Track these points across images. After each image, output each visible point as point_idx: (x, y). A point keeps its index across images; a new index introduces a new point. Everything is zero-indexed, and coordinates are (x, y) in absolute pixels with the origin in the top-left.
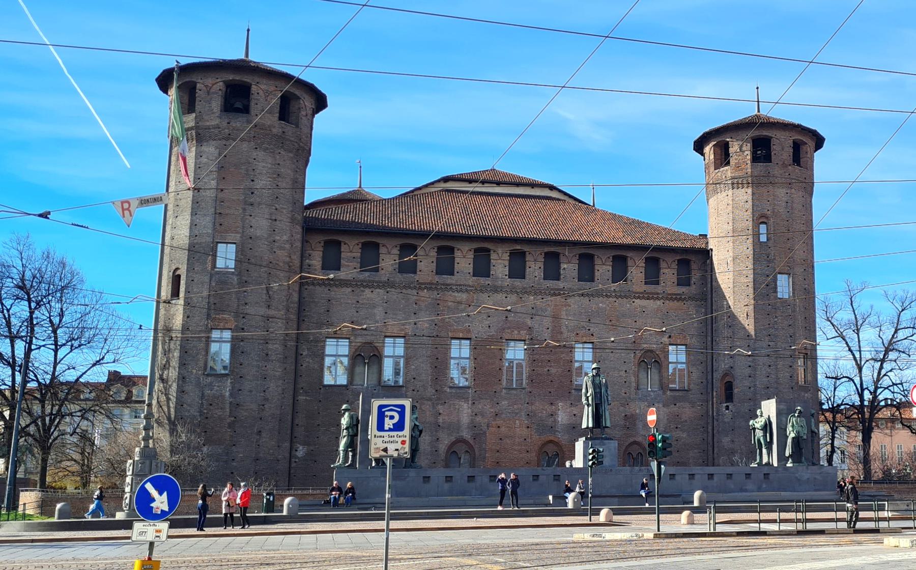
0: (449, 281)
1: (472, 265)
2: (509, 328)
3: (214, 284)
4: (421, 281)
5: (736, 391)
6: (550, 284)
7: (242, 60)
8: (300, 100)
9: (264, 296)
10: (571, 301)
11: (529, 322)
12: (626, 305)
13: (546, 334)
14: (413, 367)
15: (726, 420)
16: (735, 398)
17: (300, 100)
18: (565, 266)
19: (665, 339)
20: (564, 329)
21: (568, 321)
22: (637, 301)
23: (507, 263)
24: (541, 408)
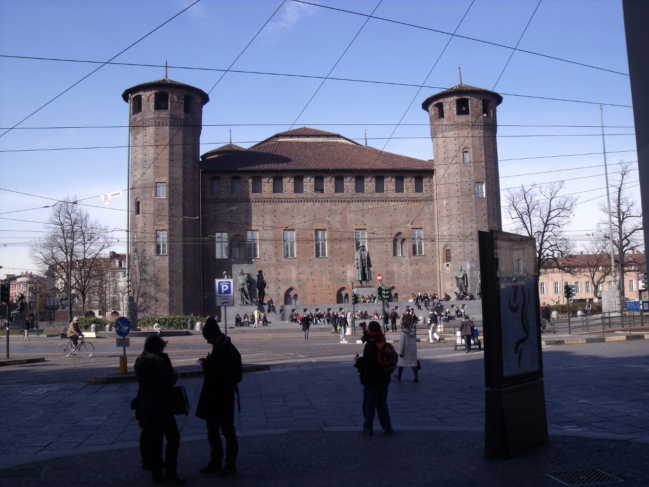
0: (281, 197)
1: (293, 187)
2: (316, 222)
5: (452, 255)
6: (338, 194)
7: (164, 80)
8: (194, 99)
10: (351, 204)
11: (328, 218)
12: (385, 204)
13: (338, 225)
15: (447, 273)
16: (452, 259)
17: (194, 99)
18: (348, 184)
19: (409, 226)
20: (349, 222)
21: (351, 216)
22: (392, 203)
23: (313, 184)
24: (338, 269)
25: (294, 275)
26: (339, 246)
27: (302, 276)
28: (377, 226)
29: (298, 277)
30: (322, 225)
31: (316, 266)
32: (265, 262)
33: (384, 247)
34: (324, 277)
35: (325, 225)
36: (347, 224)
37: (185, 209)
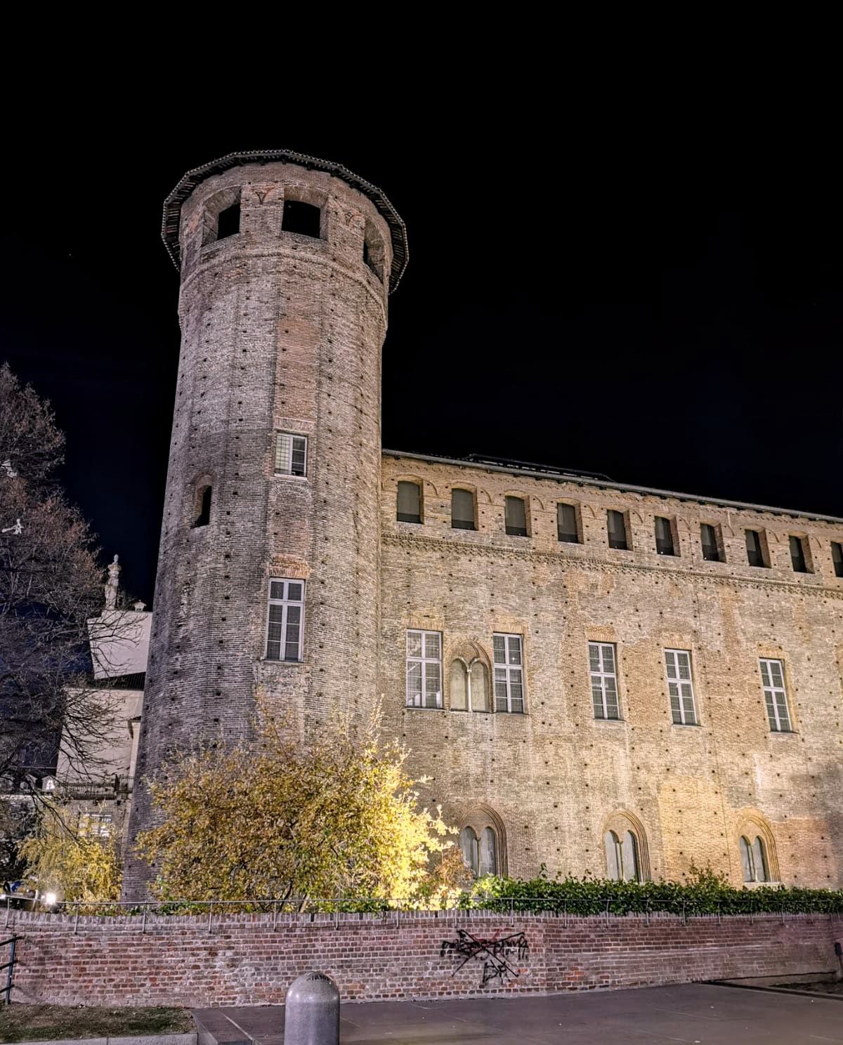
2: (666, 630)
3: (273, 499)
4: (539, 549)
9: (351, 531)
13: (718, 644)
14: (539, 684)
20: (740, 637)
22: (829, 600)
25: (624, 777)
26: (726, 698)
27: (643, 775)
28: (808, 654)
29: (634, 780)
30: (681, 639)
31: (676, 749)
32: (546, 727)
33: (831, 709)
34: (700, 783)
35: (687, 637)
36: (738, 642)
37: (359, 527)
